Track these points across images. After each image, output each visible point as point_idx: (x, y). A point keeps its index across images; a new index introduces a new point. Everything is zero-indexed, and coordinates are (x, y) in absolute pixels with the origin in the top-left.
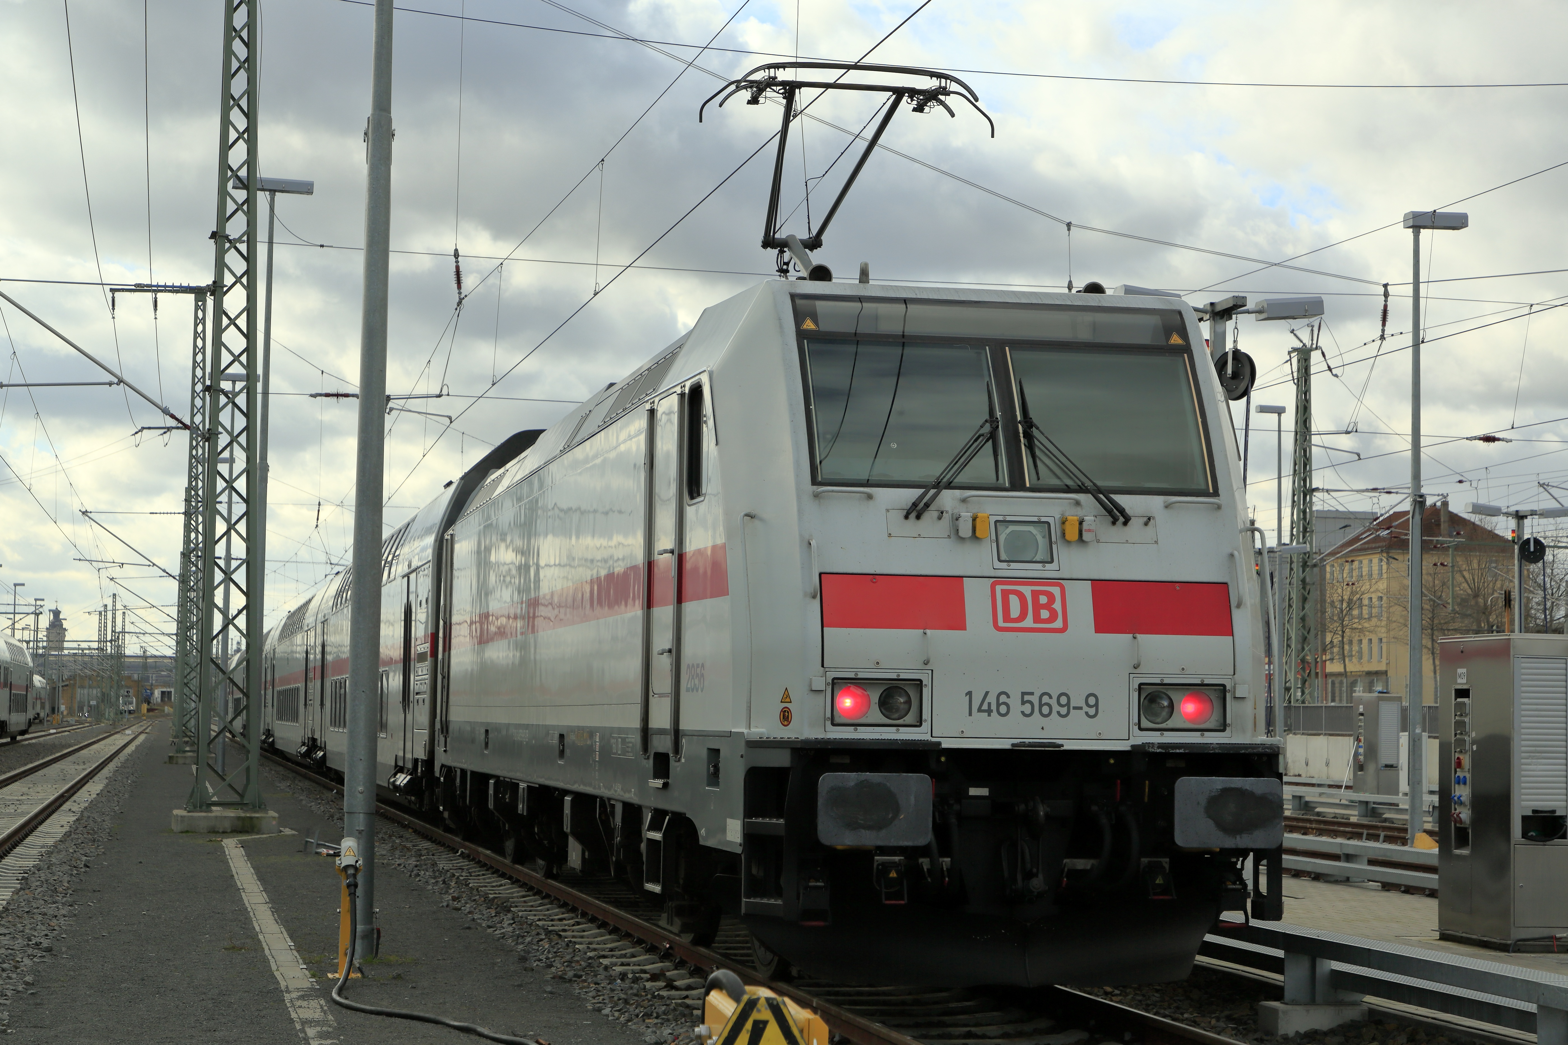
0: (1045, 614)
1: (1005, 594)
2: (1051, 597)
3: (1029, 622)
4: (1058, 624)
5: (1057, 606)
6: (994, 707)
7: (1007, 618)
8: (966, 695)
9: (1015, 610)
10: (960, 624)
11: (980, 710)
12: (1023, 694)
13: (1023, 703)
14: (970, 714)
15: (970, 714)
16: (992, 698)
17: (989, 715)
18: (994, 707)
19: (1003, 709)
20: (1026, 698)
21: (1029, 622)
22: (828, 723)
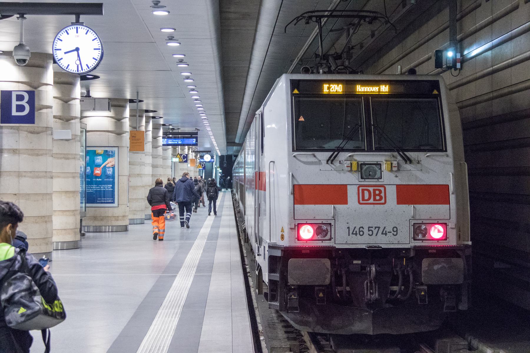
0: (378, 198)
1: (363, 190)
2: (380, 191)
3: (371, 201)
4: (383, 201)
5: (383, 194)
6: (358, 232)
7: (363, 199)
8: (347, 228)
9: (367, 196)
10: (346, 202)
11: (353, 234)
12: (369, 227)
14: (349, 235)
15: (349, 235)
16: (357, 230)
17: (356, 235)
18: (358, 232)
19: (361, 233)
20: (370, 229)
21: (371, 201)
22: (296, 240)
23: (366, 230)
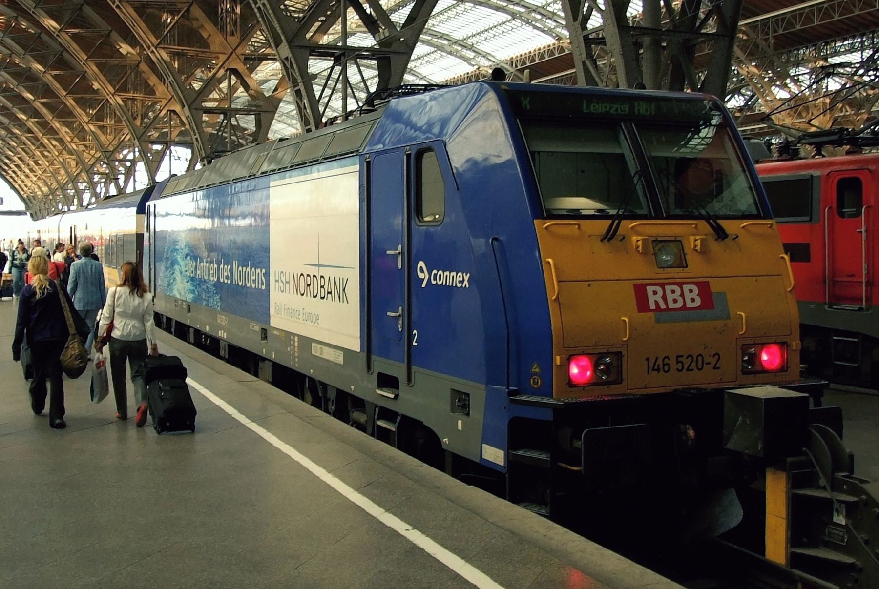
6: (661, 366)
12: (678, 357)
13: (678, 362)
14: (648, 373)
15: (648, 373)
16: (660, 362)
17: (659, 373)
18: (661, 366)
19: (666, 368)
20: (680, 359)
23: (672, 362)
